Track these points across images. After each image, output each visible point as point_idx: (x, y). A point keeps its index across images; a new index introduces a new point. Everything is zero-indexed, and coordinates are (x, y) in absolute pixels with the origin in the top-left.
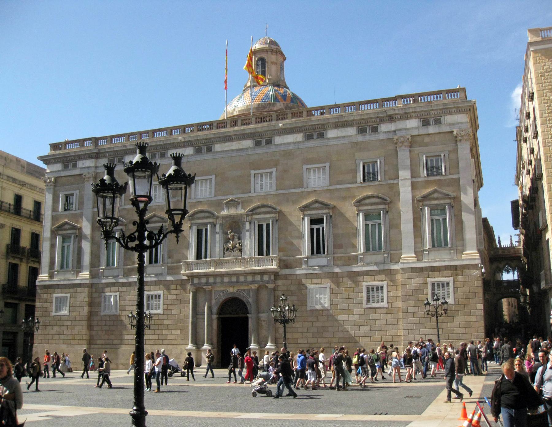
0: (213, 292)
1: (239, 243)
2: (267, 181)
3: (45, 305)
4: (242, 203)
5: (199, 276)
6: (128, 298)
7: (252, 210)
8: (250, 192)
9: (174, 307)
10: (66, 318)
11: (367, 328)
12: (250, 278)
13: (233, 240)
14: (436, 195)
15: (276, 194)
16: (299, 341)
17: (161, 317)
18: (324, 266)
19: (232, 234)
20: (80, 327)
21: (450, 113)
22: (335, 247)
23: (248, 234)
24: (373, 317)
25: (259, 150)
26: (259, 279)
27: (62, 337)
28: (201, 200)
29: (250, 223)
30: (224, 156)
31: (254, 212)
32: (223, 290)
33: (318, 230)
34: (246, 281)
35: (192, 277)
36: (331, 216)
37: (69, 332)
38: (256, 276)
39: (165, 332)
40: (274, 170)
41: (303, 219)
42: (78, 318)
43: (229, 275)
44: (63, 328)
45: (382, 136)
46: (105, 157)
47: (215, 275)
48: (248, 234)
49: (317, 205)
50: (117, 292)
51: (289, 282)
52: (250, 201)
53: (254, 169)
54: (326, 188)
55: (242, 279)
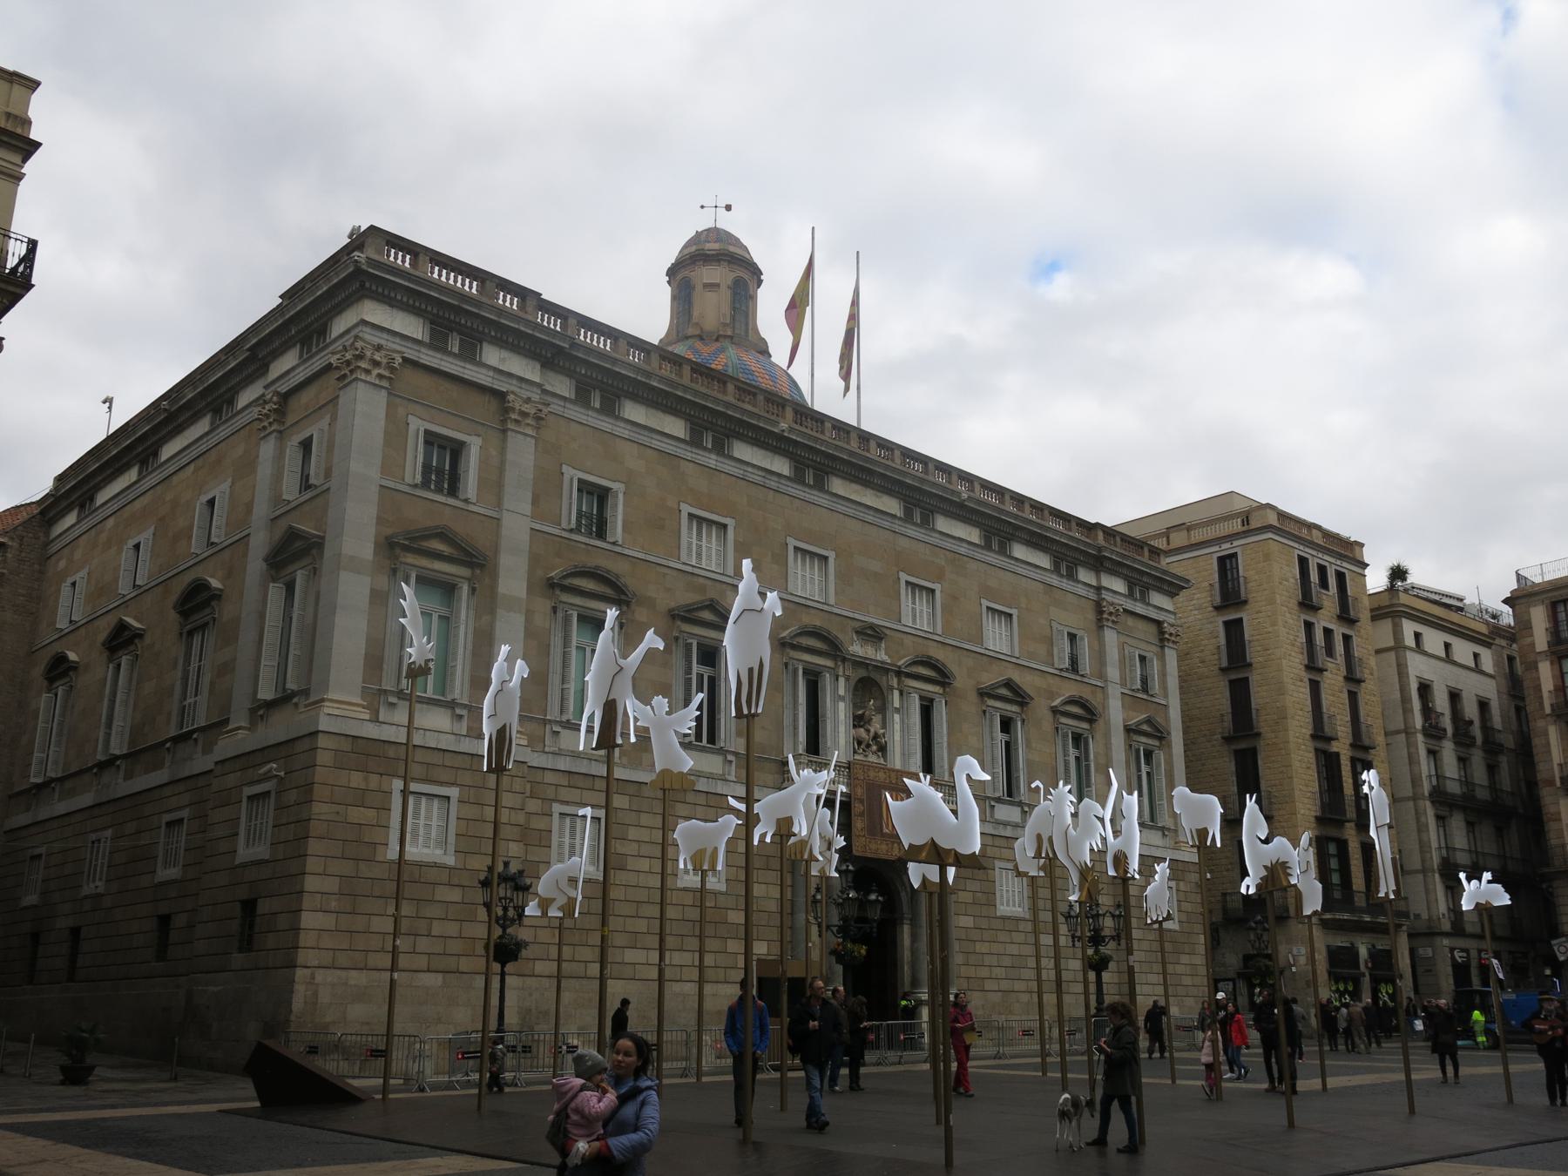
2: (922, 606)
3: (355, 814)
6: (633, 833)
14: (1145, 727)
16: (989, 985)
17: (722, 901)
21: (1160, 590)
23: (897, 717)
25: (912, 531)
29: (901, 694)
30: (850, 512)
37: (452, 929)
45: (1081, 590)
46: (569, 373)
48: (897, 717)
49: (1004, 692)
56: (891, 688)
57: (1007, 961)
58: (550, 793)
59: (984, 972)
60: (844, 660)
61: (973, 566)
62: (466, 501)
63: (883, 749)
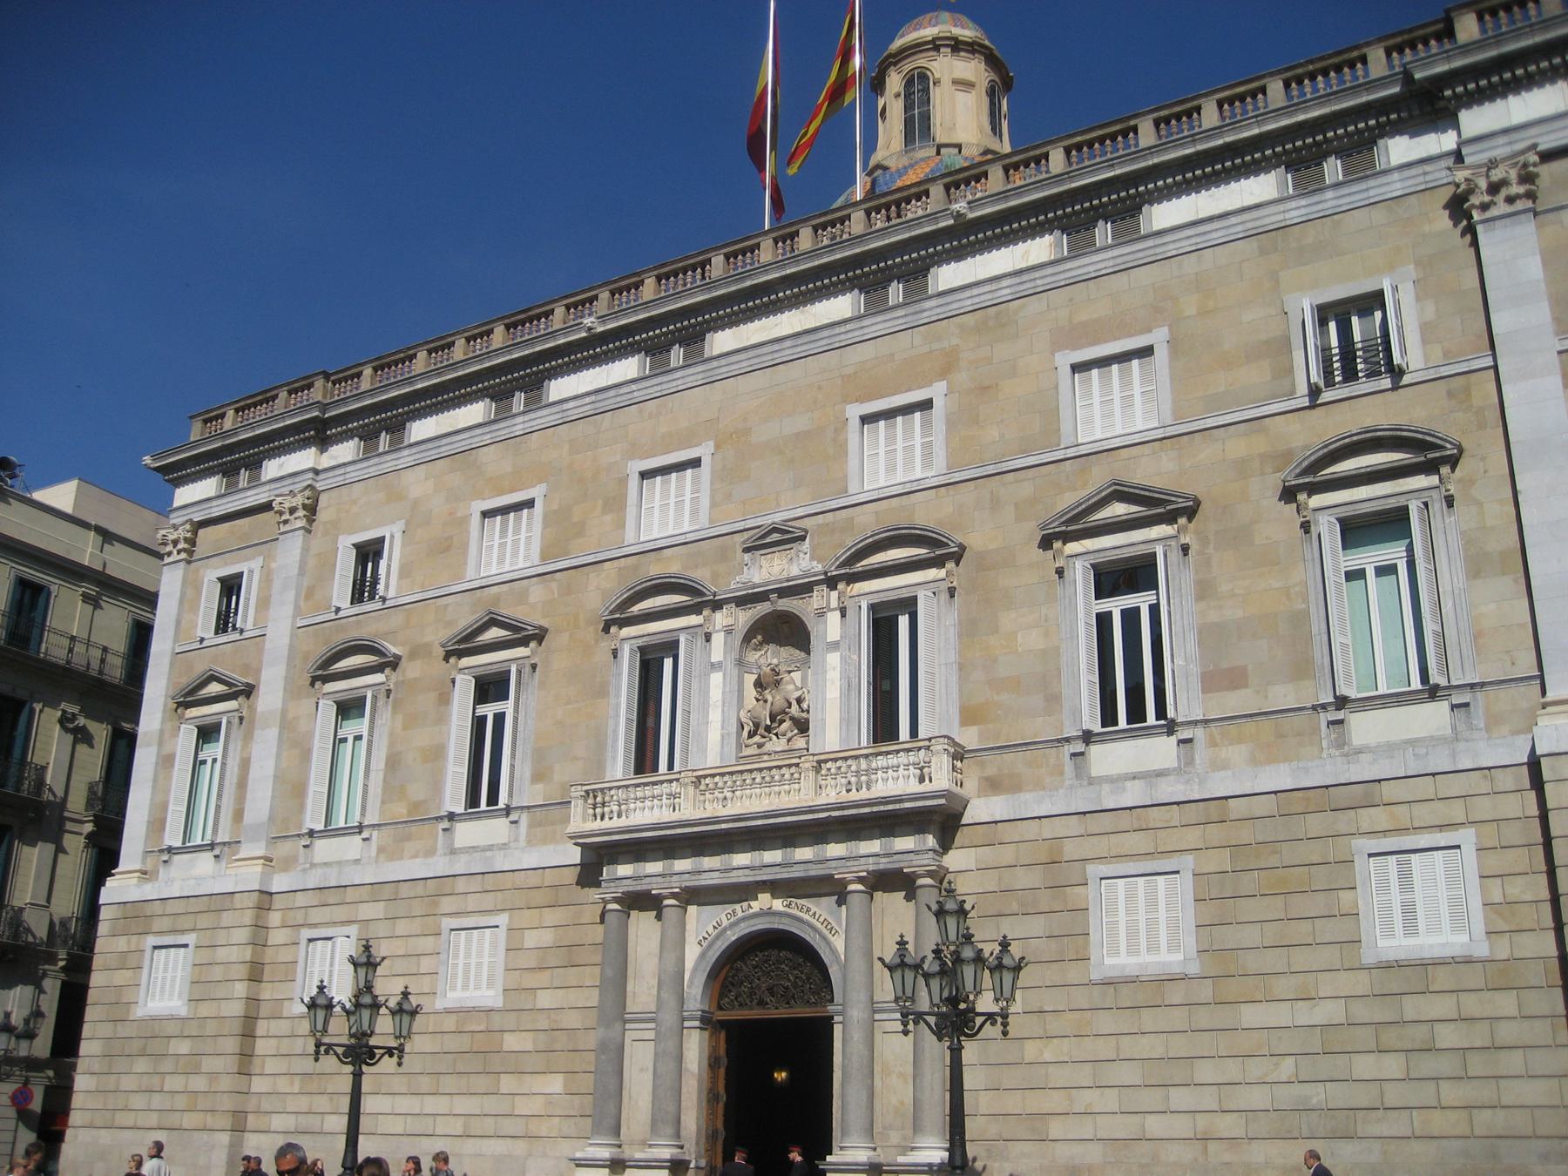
3: (121, 977)
9: (543, 978)
10: (172, 1028)
11: (1393, 1066)
16: (1056, 1129)
17: (497, 1021)
18: (1161, 774)
20: (217, 1064)
22: (1216, 680)
23: (833, 659)
24: (1413, 1007)
25: (877, 324)
27: (157, 1101)
29: (843, 615)
33: (1131, 616)
36: (1185, 549)
39: (507, 1083)
40: (937, 391)
41: (1060, 572)
42: (211, 1027)
44: (168, 1065)
45: (1395, 185)
49: (1119, 509)
50: (350, 922)
53: (860, 400)
54: (1159, 434)
56: (821, 614)
57: (1128, 1074)
58: (299, 917)
59: (1053, 1102)
60: (717, 605)
61: (1035, 305)
62: (242, 631)
63: (803, 727)
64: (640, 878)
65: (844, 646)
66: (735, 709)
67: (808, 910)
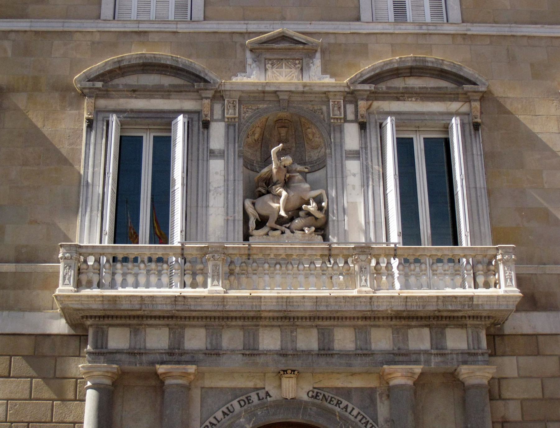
0: (196, 394)
1: (318, 200)
4: (323, 52)
5: (137, 317)
7: (377, 78)
8: (358, 19)
12: (382, 340)
13: (286, 185)
15: (464, 36)
19: (288, 160)
23: (353, 167)
26: (426, 345)
28: (143, 27)
29: (363, 126)
31: (383, 87)
32: (246, 391)
34: (364, 352)
35: (88, 324)
38: (413, 333)
43: (287, 317)
47: (217, 317)
48: (353, 167)
51: (550, 365)
52: (361, 47)
55: (344, 339)
64: (141, 354)
65: (363, 155)
66: (241, 198)
67: (339, 403)
